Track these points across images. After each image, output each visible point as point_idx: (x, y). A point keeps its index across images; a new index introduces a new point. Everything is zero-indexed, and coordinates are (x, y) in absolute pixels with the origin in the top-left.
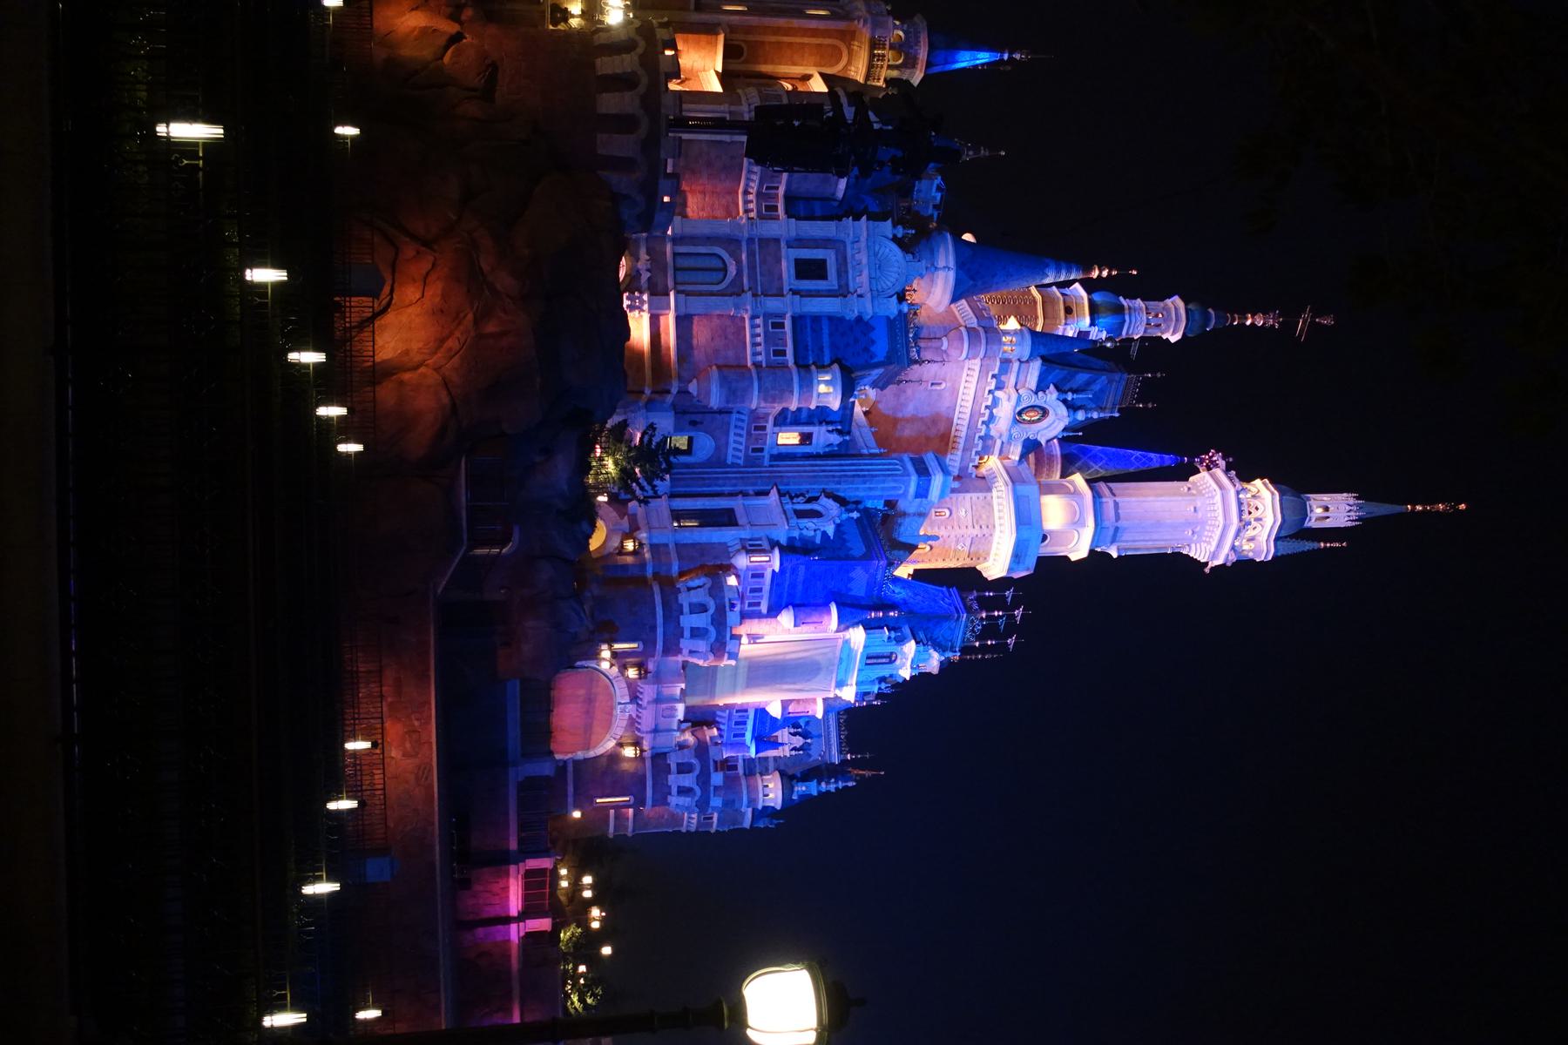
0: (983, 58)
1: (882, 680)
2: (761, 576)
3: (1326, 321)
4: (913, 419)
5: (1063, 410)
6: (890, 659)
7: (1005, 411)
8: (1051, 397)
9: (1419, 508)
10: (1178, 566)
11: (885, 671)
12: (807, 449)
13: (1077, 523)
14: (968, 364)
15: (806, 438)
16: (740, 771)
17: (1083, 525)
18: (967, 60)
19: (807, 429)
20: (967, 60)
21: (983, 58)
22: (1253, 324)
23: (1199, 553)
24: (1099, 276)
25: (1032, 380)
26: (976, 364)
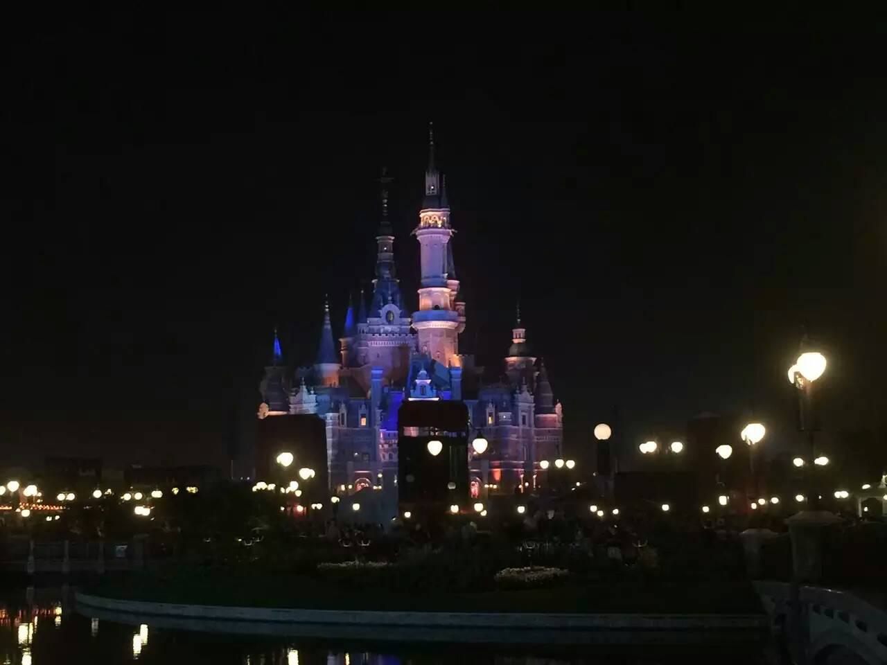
0: (277, 344)
1: (432, 389)
2: (389, 435)
3: (385, 170)
4: (393, 362)
5: (387, 306)
6: (423, 387)
7: (389, 328)
8: (383, 312)
9: (432, 143)
10: (454, 243)
11: (428, 388)
12: (367, 415)
13: (430, 294)
14: (370, 345)
15: (363, 416)
16: (497, 427)
17: (430, 291)
18: (278, 351)
19: (360, 416)
20: (278, 351)
21: (277, 344)
22: (386, 204)
23: (446, 239)
24: (328, 308)
25: (376, 319)
26: (369, 343)
